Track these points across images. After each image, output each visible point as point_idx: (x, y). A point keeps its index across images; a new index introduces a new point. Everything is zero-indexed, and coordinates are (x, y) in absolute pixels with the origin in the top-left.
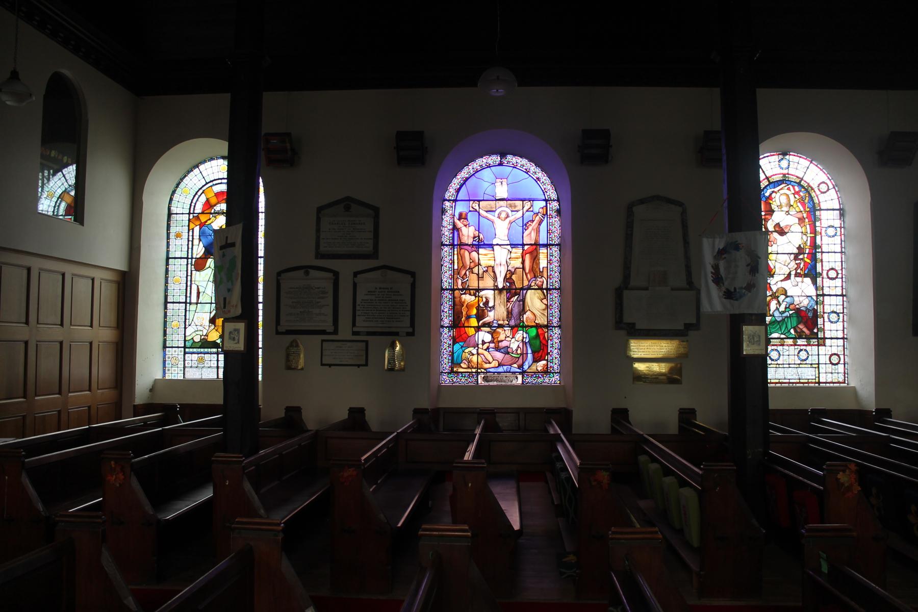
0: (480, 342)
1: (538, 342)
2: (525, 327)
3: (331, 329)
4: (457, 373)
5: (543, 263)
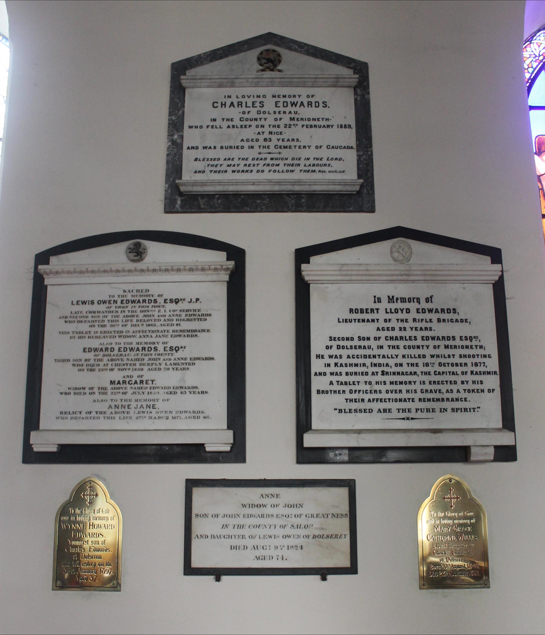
3: (220, 440)
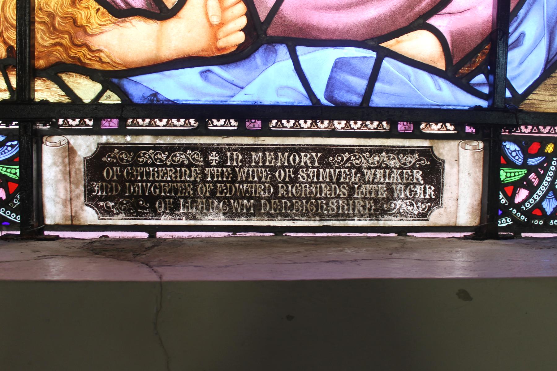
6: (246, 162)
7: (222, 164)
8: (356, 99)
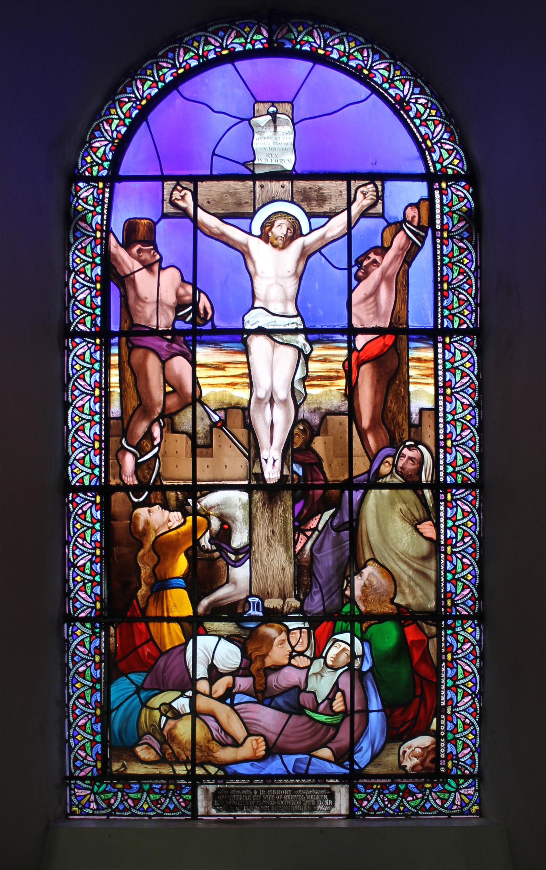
0: (202, 671)
1: (404, 672)
2: (361, 621)
4: (126, 779)
5: (421, 395)
6: (266, 793)
7: (258, 794)
8: (303, 772)
